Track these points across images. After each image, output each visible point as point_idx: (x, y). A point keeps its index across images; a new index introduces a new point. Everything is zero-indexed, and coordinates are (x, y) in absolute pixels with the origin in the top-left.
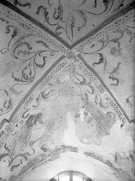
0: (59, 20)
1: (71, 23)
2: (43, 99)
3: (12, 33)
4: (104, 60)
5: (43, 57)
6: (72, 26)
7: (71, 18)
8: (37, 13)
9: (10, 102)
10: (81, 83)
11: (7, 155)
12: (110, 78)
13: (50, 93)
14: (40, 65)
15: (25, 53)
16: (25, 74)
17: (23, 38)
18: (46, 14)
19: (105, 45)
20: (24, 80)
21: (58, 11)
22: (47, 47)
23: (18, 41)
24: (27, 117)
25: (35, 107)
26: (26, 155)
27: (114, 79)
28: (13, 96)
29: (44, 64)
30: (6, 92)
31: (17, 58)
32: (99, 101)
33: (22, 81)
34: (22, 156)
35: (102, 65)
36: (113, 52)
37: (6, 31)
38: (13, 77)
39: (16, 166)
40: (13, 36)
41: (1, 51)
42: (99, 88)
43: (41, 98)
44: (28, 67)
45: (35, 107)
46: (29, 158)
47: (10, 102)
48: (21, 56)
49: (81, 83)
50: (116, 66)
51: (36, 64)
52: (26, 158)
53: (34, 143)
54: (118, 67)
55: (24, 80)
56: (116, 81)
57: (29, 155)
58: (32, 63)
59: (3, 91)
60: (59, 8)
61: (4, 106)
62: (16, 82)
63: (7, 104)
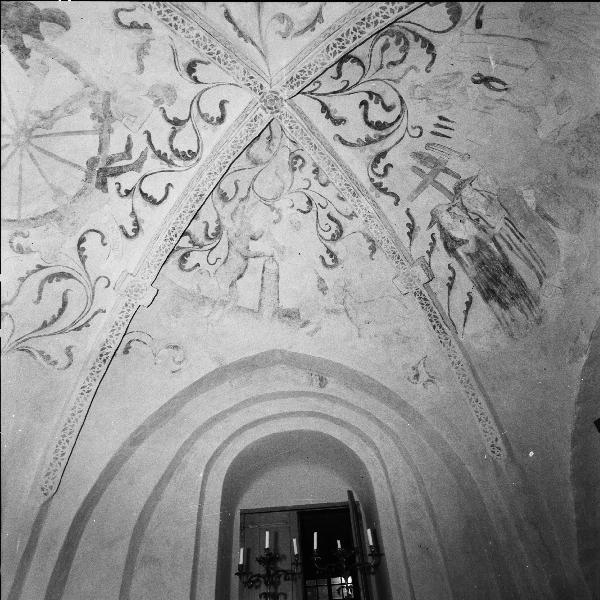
0: (297, 153)
1: (274, 141)
3: (383, 163)
5: (340, 80)
14: (352, 62)
15: (378, 98)
16: (401, 51)
17: (369, 141)
19: (195, 104)
20: (410, 37)
22: (325, 108)
23: (381, 138)
27: (133, 26)
31: (400, 97)
33: (417, 37)
35: (185, 58)
36: (171, 92)
37: (390, 170)
40: (383, 154)
41: (421, 135)
42: (175, 18)
44: (385, 63)
48: (390, 98)
50: (146, 61)
51: (364, 67)
54: (139, 60)
55: (410, 37)
56: (126, 21)
58: (373, 69)
59: (485, 28)
60: (294, 169)
62: (434, 39)
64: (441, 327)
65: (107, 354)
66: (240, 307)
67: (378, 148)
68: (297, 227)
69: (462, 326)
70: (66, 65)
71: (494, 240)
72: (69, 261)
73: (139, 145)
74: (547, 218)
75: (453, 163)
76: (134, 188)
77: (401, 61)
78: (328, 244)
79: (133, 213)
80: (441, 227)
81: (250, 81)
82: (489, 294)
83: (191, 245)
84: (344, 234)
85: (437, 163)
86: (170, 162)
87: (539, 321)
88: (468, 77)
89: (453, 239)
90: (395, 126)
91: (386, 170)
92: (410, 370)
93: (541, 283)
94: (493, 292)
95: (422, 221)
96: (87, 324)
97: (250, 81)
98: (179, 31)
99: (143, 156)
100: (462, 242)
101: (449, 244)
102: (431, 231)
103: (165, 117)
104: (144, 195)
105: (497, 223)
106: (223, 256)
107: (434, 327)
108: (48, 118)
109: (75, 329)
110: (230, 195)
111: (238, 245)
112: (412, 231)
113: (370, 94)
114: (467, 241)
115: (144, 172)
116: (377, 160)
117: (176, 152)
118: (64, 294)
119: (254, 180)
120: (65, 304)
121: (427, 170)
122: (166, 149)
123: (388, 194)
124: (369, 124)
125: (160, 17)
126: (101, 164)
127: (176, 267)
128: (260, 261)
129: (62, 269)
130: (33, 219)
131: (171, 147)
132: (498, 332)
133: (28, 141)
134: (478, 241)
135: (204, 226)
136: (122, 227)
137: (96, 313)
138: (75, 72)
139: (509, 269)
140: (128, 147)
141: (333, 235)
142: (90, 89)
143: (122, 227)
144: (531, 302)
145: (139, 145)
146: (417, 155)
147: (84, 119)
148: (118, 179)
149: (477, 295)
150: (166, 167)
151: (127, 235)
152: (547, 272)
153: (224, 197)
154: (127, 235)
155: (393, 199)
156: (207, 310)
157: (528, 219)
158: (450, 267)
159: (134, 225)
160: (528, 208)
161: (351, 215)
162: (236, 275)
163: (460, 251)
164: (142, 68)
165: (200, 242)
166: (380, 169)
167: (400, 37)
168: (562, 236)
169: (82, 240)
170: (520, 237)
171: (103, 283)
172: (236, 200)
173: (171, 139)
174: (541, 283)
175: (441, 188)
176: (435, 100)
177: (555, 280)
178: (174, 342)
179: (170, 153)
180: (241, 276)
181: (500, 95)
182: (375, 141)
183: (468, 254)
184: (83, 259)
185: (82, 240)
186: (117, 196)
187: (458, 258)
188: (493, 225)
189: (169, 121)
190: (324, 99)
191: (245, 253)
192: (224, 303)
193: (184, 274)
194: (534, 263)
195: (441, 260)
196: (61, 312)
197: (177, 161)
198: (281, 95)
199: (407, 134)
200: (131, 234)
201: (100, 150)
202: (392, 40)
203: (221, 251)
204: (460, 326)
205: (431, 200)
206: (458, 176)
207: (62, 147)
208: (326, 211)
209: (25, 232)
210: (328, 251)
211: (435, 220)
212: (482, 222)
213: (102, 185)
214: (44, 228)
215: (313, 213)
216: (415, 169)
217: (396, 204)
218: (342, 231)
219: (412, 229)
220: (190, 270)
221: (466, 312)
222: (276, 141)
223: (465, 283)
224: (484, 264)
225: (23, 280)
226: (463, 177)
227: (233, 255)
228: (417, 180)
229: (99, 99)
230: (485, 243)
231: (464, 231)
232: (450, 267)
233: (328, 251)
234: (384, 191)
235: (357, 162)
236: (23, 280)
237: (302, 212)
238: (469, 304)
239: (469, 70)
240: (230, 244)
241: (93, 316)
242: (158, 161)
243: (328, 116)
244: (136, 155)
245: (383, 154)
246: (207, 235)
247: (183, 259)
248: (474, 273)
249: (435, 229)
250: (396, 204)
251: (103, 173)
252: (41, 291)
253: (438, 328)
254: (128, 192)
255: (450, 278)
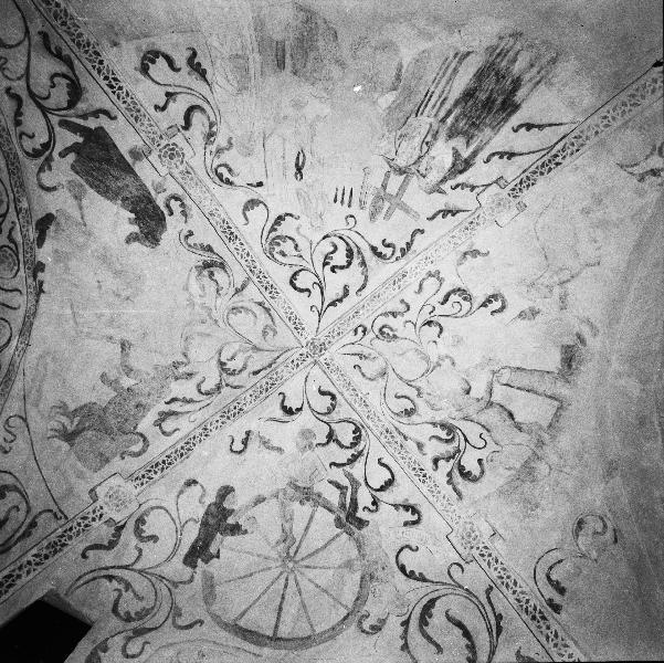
0: (377, 333)
2: (200, 264)
3: (381, 249)
4: (287, 418)
6: (361, 356)
7: (374, 354)
8: (402, 301)
9: (228, 182)
10: (222, 364)
11: (72, 104)
12: (248, 433)
13: (213, 284)
18: (394, 314)
20: (273, 235)
21: (391, 333)
22: (333, 304)
23: (359, 252)
24: (168, 206)
25: (187, 237)
26: (43, 158)
27: (245, 442)
28: (242, 196)
29: (295, 288)
30: (260, 184)
32: (175, 407)
33: (273, 229)
34: (46, 146)
35: (279, 414)
36: (306, 434)
37: (387, 242)
38: (287, 214)
39: (18, 113)
40: (374, 249)
43: (207, 257)
45: (187, 237)
46: (31, 166)
47: (228, 182)
49: (222, 364)
50: (275, 443)
52: (36, 154)
53: (76, 197)
55: (273, 235)
56: (241, 447)
57: (41, 170)
60: (395, 336)
61: (226, 166)
63: (226, 175)
64: (556, 156)
65: (535, 609)
66: (550, 425)
67: (368, 254)
68: (458, 341)
69: (562, 127)
70: (256, 504)
71: (443, 121)
72: (416, 593)
73: (338, 475)
74: (398, 77)
75: (376, 180)
76: (373, 497)
77: (293, 240)
78: (475, 306)
79: (396, 506)
80: (444, 180)
81: (295, 363)
82: (509, 107)
83: (452, 461)
84: (463, 287)
85: (379, 198)
86: (360, 453)
87: (516, 35)
88: (298, 184)
89: (454, 165)
90: (348, 240)
91: (388, 246)
92: (645, 186)
93: (468, 53)
94: (504, 102)
95: (439, 202)
96: (499, 617)
97: (295, 363)
98: (245, 408)
99: (349, 476)
100: (456, 154)
101: (461, 168)
102: (449, 191)
103: (323, 445)
104: (382, 489)
105: (425, 121)
106: (479, 429)
107: (558, 164)
108: (286, 537)
109: (498, 636)
110: (409, 406)
111: (471, 412)
112: (450, 211)
113: (325, 264)
114: (453, 148)
115: (362, 481)
116: (379, 255)
117: (353, 445)
118: (449, 618)
119: (401, 379)
120: (460, 625)
121: (387, 205)
122: (349, 453)
123: (412, 241)
124: (349, 264)
125: (232, 418)
126: (343, 516)
127: (471, 485)
128: (498, 389)
129: (421, 605)
130: (357, 599)
131: (348, 448)
132: (555, 80)
133: (296, 562)
134: (450, 136)
135: (434, 440)
136: (406, 524)
137: (488, 598)
138: (264, 499)
139: (469, 94)
140: (338, 486)
141: (465, 299)
142: (281, 494)
143: (406, 524)
144: (499, 55)
145: (338, 475)
146: (373, 216)
147: (301, 511)
148: (360, 507)
149: (515, 120)
150: (363, 458)
151: (414, 523)
152: (452, 55)
153: (409, 413)
154: (414, 523)
155: (418, 236)
156: (542, 468)
157: (409, 92)
158: (488, 161)
159: (407, 510)
160: (398, 98)
161: (438, 278)
162: (509, 422)
163: (465, 154)
164: (280, 450)
165: (452, 451)
166: (388, 251)
167: (275, 242)
168: (407, 55)
169: (402, 569)
170: (428, 95)
171: (456, 572)
172: (417, 400)
173: (342, 446)
174: (468, 53)
175: (402, 188)
176: (320, 208)
177: (458, 42)
178: (571, 525)
179: (352, 451)
180: (511, 415)
181: (308, 155)
182: (363, 257)
183: (468, 143)
184: (422, 579)
185: (402, 569)
186: (375, 515)
187: (475, 154)
188: (428, 126)
189: (328, 443)
190: (326, 304)
191: (483, 404)
192: (541, 443)
193: (484, 479)
194: (450, 71)
195: (479, 173)
196: (467, 634)
197: (360, 447)
198: (309, 338)
199: (355, 229)
200: (415, 517)
201: (330, 511)
202: (277, 249)
203: (472, 431)
204: (562, 130)
205: (419, 199)
206: (387, 175)
207: (316, 539)
208: (438, 306)
209: (364, 613)
210: (484, 305)
211: (437, 189)
212: (429, 139)
213: (361, 523)
214: (371, 596)
215: (442, 321)
216: (388, 216)
217: (422, 232)
218: (459, 290)
219: (448, 212)
220: (483, 472)
221: (540, 127)
222: (366, 352)
223: (504, 138)
224: (473, 123)
225: (405, 647)
226: (387, 168)
227: (483, 418)
228: (398, 213)
229: (290, 491)
230: (450, 129)
231: (443, 154)
232: (488, 161)
233: (484, 305)
234: (409, 245)
235: (381, 272)
236: (405, 647)
237: (441, 332)
238: (529, 127)
239: (294, 184)
240: (465, 419)
241: (490, 602)
242: (356, 464)
243: (340, 300)
244: (345, 482)
245: (374, 249)
246: (447, 441)
247: (465, 475)
248: (488, 131)
249: (446, 187)
250: (422, 232)
251: (350, 518)
252: (429, 639)
253: (558, 160)
254: (374, 503)
255: (501, 157)
